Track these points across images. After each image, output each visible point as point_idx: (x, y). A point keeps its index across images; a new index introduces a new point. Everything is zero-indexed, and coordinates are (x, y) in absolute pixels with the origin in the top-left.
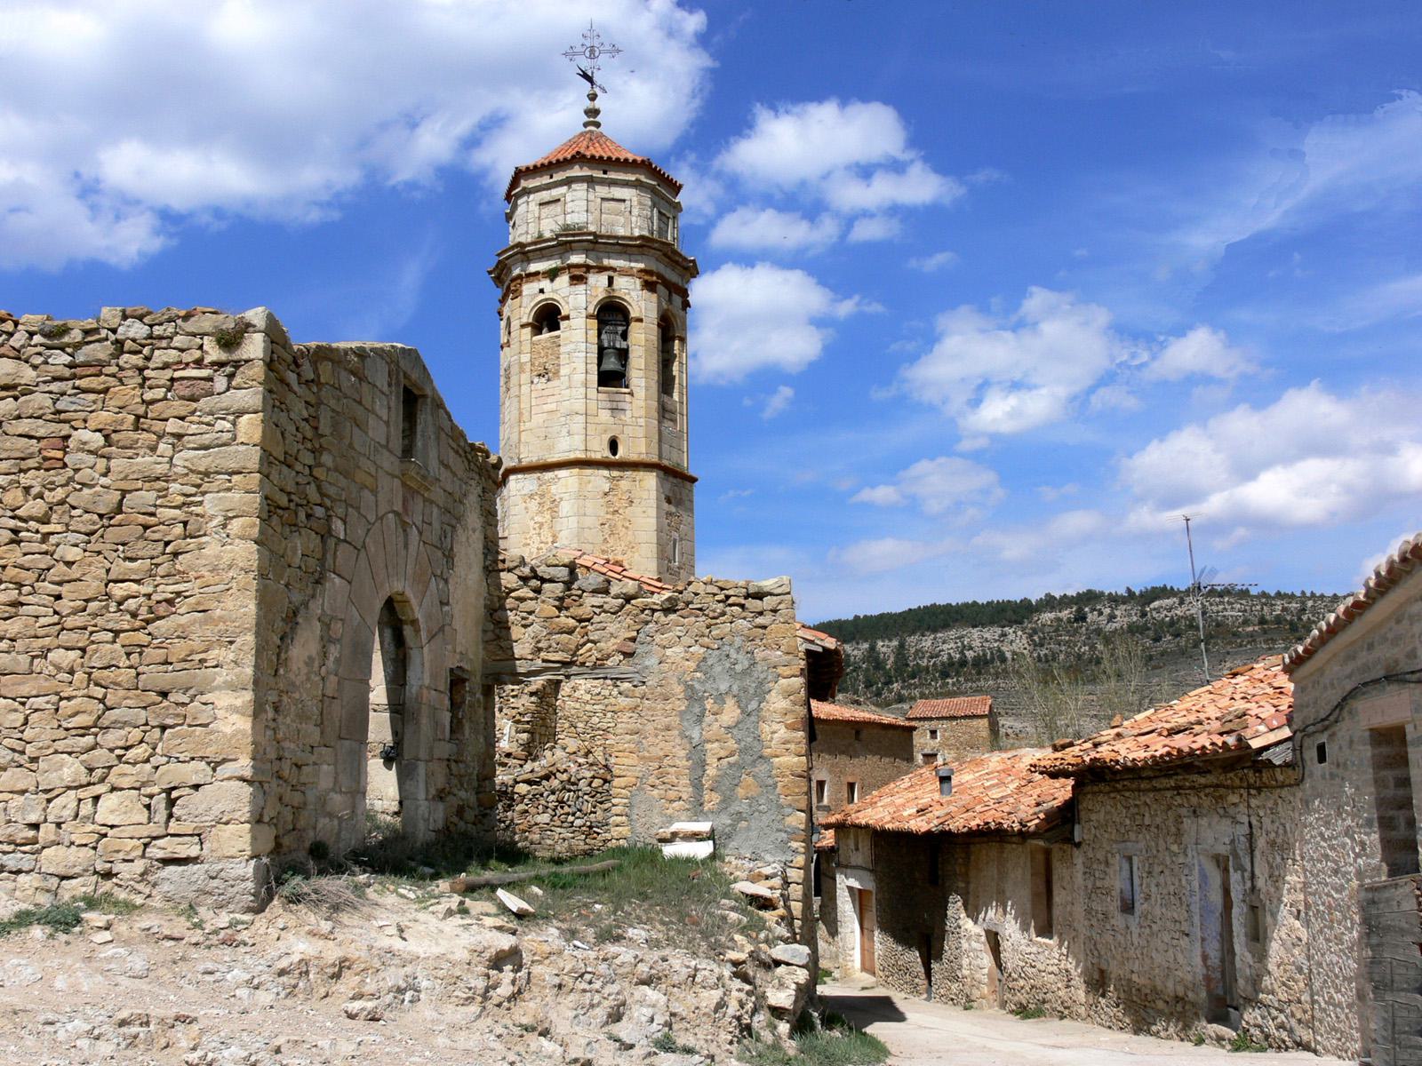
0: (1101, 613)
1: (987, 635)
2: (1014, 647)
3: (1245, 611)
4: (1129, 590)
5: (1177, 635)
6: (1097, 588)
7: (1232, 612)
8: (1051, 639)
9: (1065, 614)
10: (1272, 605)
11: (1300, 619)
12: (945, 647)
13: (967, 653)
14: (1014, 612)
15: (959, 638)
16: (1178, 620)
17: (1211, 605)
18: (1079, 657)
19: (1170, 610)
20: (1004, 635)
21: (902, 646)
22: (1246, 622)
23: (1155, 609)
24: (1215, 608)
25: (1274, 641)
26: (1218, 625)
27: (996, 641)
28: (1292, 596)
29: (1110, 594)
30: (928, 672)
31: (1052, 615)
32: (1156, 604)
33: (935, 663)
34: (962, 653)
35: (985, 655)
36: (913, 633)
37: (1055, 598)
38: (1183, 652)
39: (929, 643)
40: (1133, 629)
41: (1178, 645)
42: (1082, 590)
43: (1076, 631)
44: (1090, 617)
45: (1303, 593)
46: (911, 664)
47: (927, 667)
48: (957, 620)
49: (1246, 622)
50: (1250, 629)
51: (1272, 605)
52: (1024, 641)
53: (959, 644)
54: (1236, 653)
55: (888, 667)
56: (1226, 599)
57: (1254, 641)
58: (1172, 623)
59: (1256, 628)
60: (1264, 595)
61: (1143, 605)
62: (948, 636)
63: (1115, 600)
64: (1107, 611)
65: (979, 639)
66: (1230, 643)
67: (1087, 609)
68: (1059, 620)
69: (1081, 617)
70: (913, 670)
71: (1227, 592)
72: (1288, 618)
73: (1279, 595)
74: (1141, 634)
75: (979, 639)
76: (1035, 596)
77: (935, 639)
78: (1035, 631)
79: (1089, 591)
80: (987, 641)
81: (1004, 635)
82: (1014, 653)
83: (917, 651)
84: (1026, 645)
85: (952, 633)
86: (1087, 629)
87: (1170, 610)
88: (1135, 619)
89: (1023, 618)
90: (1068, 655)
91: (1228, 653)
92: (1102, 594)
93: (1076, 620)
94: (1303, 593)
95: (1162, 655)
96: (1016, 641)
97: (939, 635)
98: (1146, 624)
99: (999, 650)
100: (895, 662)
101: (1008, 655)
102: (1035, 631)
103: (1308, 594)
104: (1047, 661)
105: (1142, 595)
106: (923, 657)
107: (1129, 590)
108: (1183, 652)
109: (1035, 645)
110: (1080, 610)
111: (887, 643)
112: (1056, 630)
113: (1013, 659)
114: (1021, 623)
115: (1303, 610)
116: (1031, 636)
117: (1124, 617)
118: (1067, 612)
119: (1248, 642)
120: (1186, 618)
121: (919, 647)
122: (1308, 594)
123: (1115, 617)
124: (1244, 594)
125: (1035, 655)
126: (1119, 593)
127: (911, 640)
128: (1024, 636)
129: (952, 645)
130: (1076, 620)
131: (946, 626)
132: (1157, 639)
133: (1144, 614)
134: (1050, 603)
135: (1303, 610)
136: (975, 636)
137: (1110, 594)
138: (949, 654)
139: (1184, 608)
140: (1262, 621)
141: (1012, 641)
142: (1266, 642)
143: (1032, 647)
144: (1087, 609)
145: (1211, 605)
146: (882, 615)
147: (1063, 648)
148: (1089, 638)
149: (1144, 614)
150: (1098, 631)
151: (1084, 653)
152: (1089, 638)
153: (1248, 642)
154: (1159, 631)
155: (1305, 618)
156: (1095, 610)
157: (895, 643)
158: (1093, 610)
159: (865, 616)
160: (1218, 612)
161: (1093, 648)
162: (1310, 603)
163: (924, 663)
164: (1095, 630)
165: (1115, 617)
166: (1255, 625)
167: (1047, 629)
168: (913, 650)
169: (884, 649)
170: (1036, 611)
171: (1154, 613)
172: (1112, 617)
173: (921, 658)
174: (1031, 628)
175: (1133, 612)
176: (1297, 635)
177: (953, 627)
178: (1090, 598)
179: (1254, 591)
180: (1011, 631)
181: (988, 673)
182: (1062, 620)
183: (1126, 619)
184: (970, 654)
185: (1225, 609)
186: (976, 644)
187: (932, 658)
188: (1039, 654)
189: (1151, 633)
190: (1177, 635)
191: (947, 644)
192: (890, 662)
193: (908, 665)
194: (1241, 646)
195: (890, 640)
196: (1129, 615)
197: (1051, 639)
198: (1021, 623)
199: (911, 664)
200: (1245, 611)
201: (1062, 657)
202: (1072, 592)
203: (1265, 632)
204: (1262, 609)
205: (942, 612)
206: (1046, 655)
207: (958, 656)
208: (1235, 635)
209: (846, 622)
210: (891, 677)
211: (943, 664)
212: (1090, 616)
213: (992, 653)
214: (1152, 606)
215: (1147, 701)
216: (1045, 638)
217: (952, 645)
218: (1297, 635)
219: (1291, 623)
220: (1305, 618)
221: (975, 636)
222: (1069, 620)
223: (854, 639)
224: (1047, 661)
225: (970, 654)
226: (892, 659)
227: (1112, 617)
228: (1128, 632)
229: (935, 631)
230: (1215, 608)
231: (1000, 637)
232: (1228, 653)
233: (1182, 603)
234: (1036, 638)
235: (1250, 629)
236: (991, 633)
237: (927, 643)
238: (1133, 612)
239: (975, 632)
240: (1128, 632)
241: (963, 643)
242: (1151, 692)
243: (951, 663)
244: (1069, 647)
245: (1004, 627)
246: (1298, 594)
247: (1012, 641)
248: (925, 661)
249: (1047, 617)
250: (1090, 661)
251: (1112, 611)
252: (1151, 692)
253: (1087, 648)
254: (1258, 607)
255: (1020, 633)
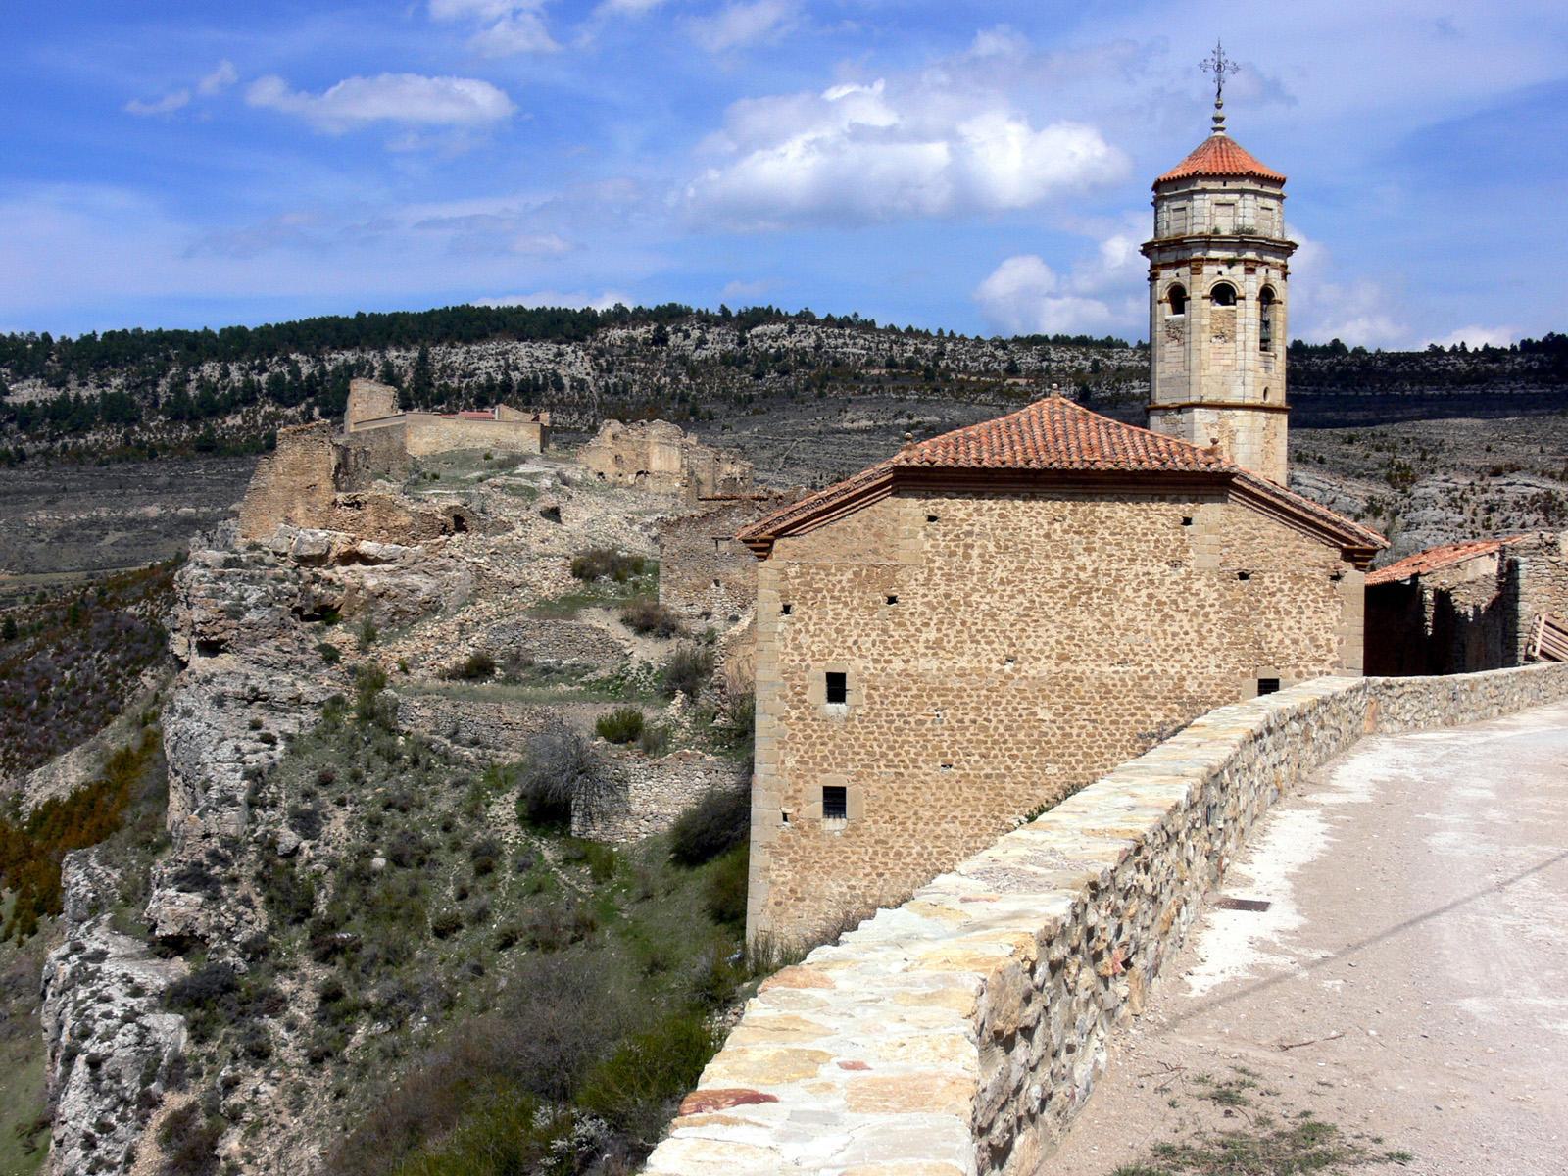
0: (687, 336)
1: (538, 353)
2: (574, 371)
3: (870, 348)
4: (724, 309)
5: (784, 372)
6: (682, 300)
7: (854, 349)
8: (622, 364)
9: (641, 333)
10: (903, 344)
11: (936, 365)
12: (483, 364)
13: (512, 374)
14: (574, 324)
15: (500, 353)
16: (787, 352)
17: (828, 337)
18: (659, 390)
19: (776, 339)
20: (560, 354)
21: (423, 358)
22: (870, 364)
23: (757, 336)
24: (832, 342)
25: (905, 390)
26: (836, 364)
27: (550, 361)
28: (927, 335)
29: (699, 311)
30: (459, 396)
31: (623, 333)
32: (759, 330)
33: (468, 385)
34: (506, 374)
35: (536, 378)
36: (438, 342)
37: (626, 309)
38: (791, 395)
39: (460, 358)
40: (727, 359)
41: (785, 386)
42: (664, 302)
43: (654, 355)
44: (673, 340)
45: (940, 331)
46: (437, 384)
47: (459, 390)
48: (497, 330)
49: (870, 364)
50: (876, 372)
51: (903, 344)
52: (587, 364)
53: (502, 362)
54: (860, 401)
55: (405, 385)
56: (847, 332)
57: (881, 388)
58: (779, 356)
59: (883, 372)
60: (892, 329)
61: (742, 331)
62: (486, 350)
63: (705, 320)
64: (696, 334)
65: (529, 356)
66: (852, 388)
67: (669, 329)
68: (632, 340)
69: (661, 339)
70: (440, 392)
71: (843, 323)
72: (923, 362)
73: (910, 330)
74: (738, 367)
75: (529, 356)
76: (603, 305)
77: (468, 352)
78: (601, 352)
79: (673, 306)
80: (538, 360)
81: (560, 354)
82: (573, 379)
83: (444, 367)
84: (589, 370)
85: (492, 347)
86: (668, 355)
87: (776, 339)
88: (731, 346)
89: (586, 333)
90: (644, 386)
91: (850, 401)
92: (688, 311)
93: (655, 342)
94: (940, 331)
95: (765, 397)
96: (576, 364)
97: (474, 348)
98: (744, 354)
99: (554, 373)
100: (415, 380)
101: (566, 381)
102: (601, 352)
103: (946, 335)
104: (616, 393)
105: (740, 315)
106: (453, 376)
107: (724, 309)
108: (791, 395)
109: (601, 371)
110: (660, 329)
111: (403, 353)
112: (629, 353)
113: (572, 387)
114: (583, 340)
115: (941, 354)
116: (595, 358)
117: (718, 343)
118: (642, 330)
119: (874, 389)
120: (796, 352)
121: (447, 361)
122: (946, 335)
123: (705, 342)
124: (868, 326)
125: (602, 384)
126: (710, 312)
127: (437, 352)
128: (587, 358)
129: (492, 362)
130: (655, 342)
131: (482, 337)
132: (758, 376)
133: (742, 342)
134: (619, 316)
135: (941, 354)
136: (523, 352)
137: (699, 311)
138: (488, 374)
139: (794, 338)
140: (891, 364)
141: (571, 364)
142: (895, 390)
143: (597, 373)
144: (669, 329)
145: (828, 337)
146: (395, 316)
147: (637, 377)
148: (671, 367)
149: (742, 342)
150: (683, 359)
151: (665, 386)
152: (671, 367)
153: (874, 389)
154: (762, 363)
155: (942, 364)
156: (680, 331)
157: (414, 354)
158: (676, 331)
159: (372, 314)
160: (836, 347)
161: (676, 379)
162: (949, 346)
163: (454, 383)
164: (680, 357)
165: (705, 342)
166: (881, 368)
167: (616, 351)
168: (438, 365)
169: (399, 361)
170: (602, 326)
171: (756, 341)
172: (701, 343)
173: (449, 377)
174: (596, 348)
175: (729, 338)
176: (933, 384)
177: (493, 339)
178: (673, 314)
179: (880, 325)
180: (570, 349)
181: (539, 403)
182: (635, 340)
183: (719, 347)
184: (516, 376)
185: (845, 344)
186: (524, 363)
187: (464, 377)
188: (607, 384)
189: (752, 367)
190: (784, 372)
191: (485, 360)
192: (407, 379)
193: (432, 385)
194: (865, 393)
195: (408, 350)
196: (724, 342)
197: (622, 364)
198: (583, 340)
199: (437, 384)
200: (870, 348)
201: (636, 388)
202: (649, 304)
203: (894, 377)
204: (891, 347)
205: (478, 318)
206: (615, 385)
207: (500, 378)
208: (856, 377)
209: (346, 319)
210: (409, 399)
211: (480, 386)
212: (672, 338)
213: (545, 377)
214: (753, 332)
215: (782, 459)
216: (613, 362)
217: (492, 362)
218: (933, 384)
219: (927, 370)
220: (942, 364)
221: (523, 352)
222: (645, 342)
223: (357, 344)
224: (616, 393)
225: (516, 376)
226: (410, 375)
227: (701, 343)
228: (722, 363)
229: (468, 341)
230: (832, 342)
231: (556, 355)
232: (850, 401)
233: (791, 332)
234: (602, 361)
235: (876, 372)
236: (544, 350)
237: (458, 356)
238: (729, 338)
239: (523, 348)
240: (722, 363)
241: (506, 360)
242: (786, 449)
243: (490, 386)
244: (645, 376)
245: (560, 343)
246: (934, 333)
247: (571, 364)
248: (456, 380)
249: (617, 334)
250: (673, 398)
251: (703, 333)
252: (786, 449)
253: (668, 380)
254: (886, 346)
255: (581, 353)
